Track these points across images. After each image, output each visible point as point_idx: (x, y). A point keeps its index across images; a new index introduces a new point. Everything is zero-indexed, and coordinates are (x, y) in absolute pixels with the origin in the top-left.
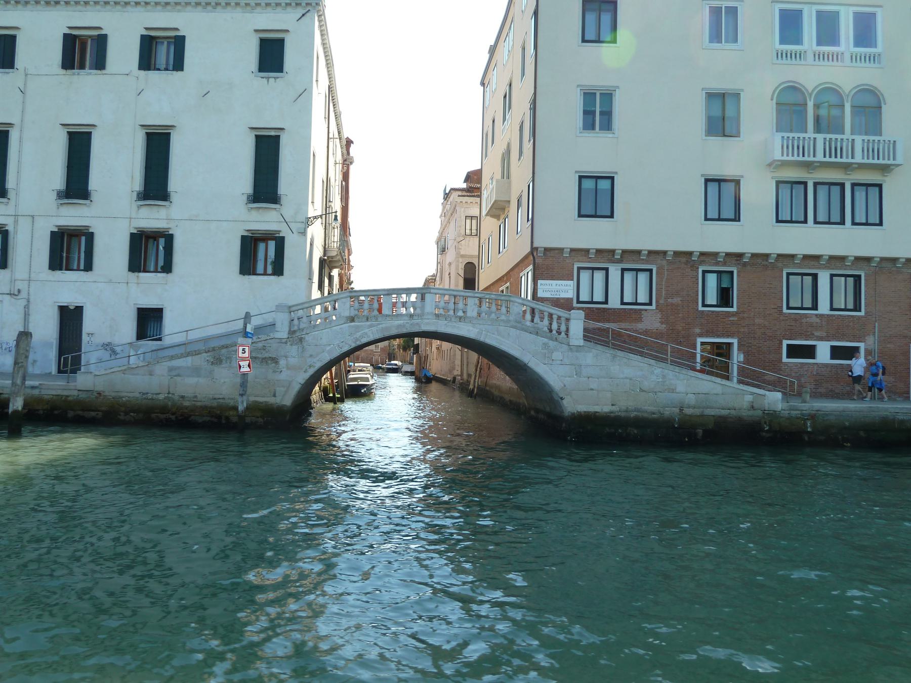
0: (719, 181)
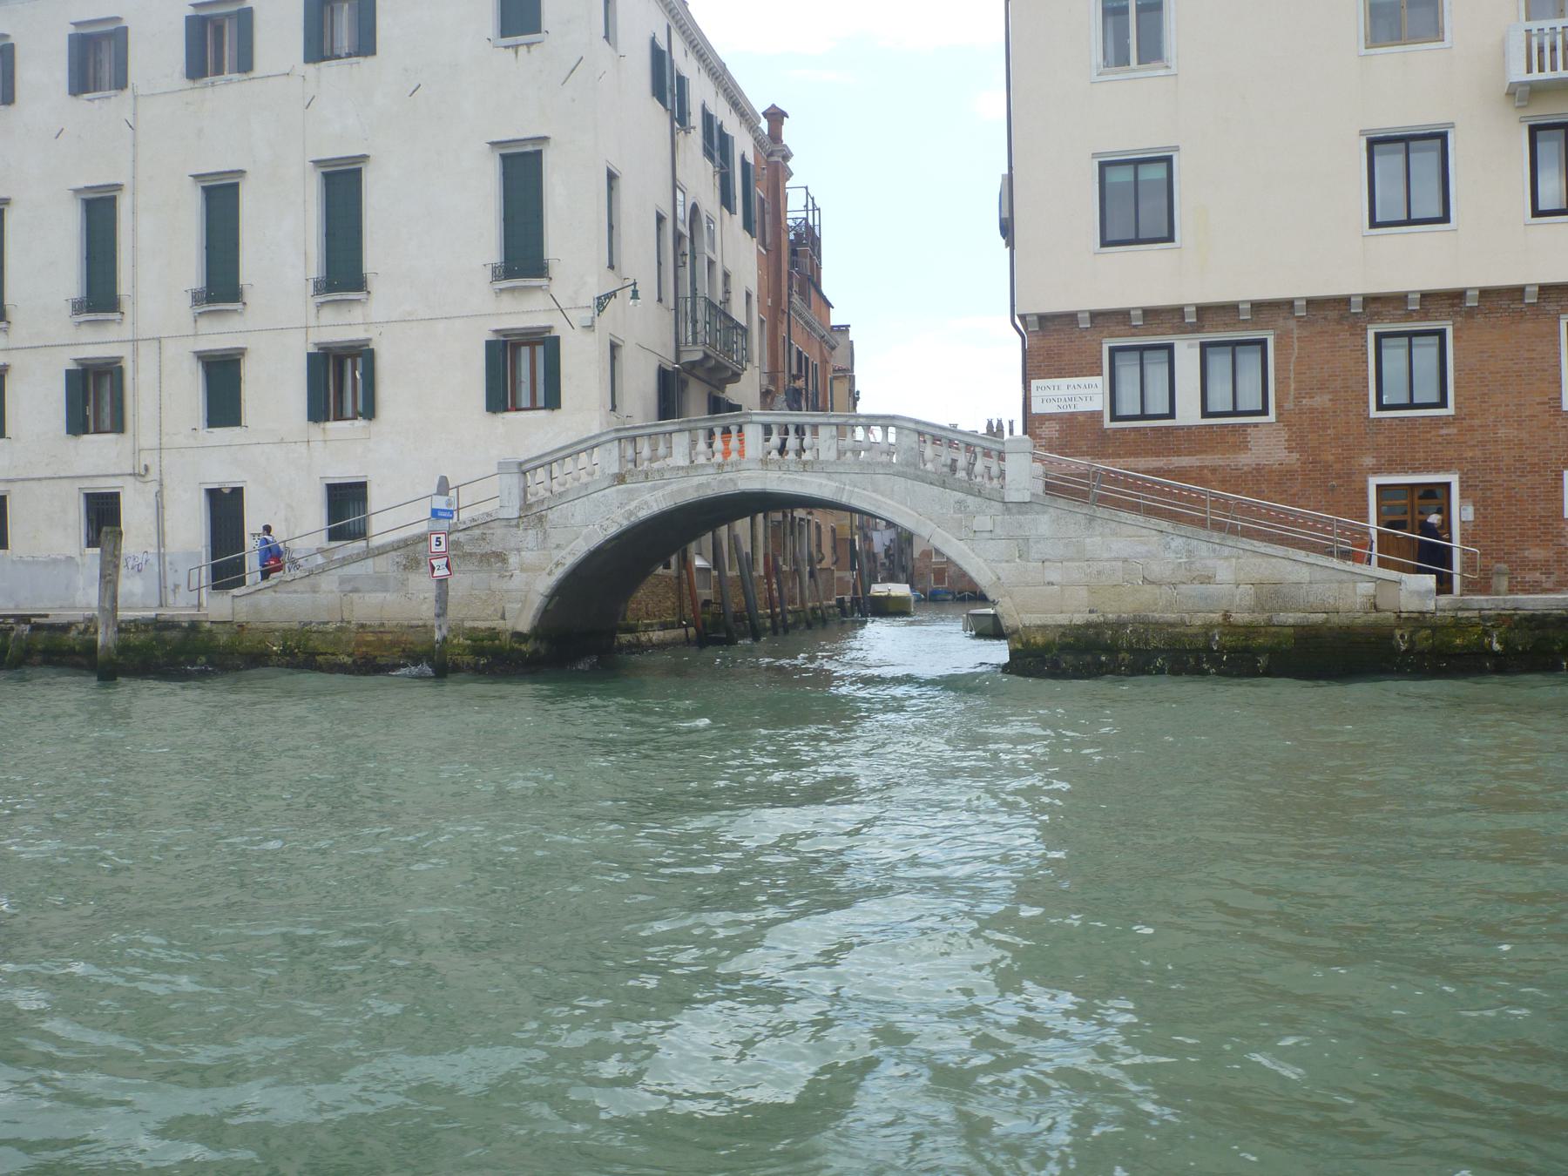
0: (1405, 140)
